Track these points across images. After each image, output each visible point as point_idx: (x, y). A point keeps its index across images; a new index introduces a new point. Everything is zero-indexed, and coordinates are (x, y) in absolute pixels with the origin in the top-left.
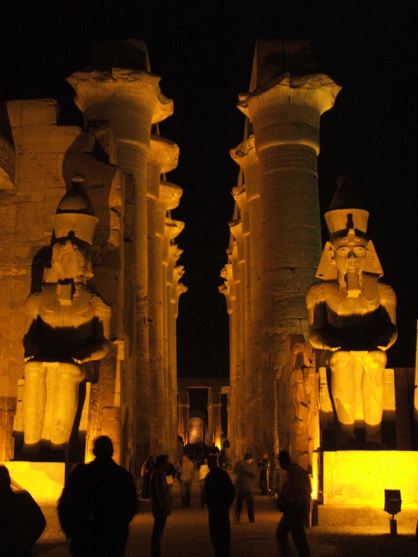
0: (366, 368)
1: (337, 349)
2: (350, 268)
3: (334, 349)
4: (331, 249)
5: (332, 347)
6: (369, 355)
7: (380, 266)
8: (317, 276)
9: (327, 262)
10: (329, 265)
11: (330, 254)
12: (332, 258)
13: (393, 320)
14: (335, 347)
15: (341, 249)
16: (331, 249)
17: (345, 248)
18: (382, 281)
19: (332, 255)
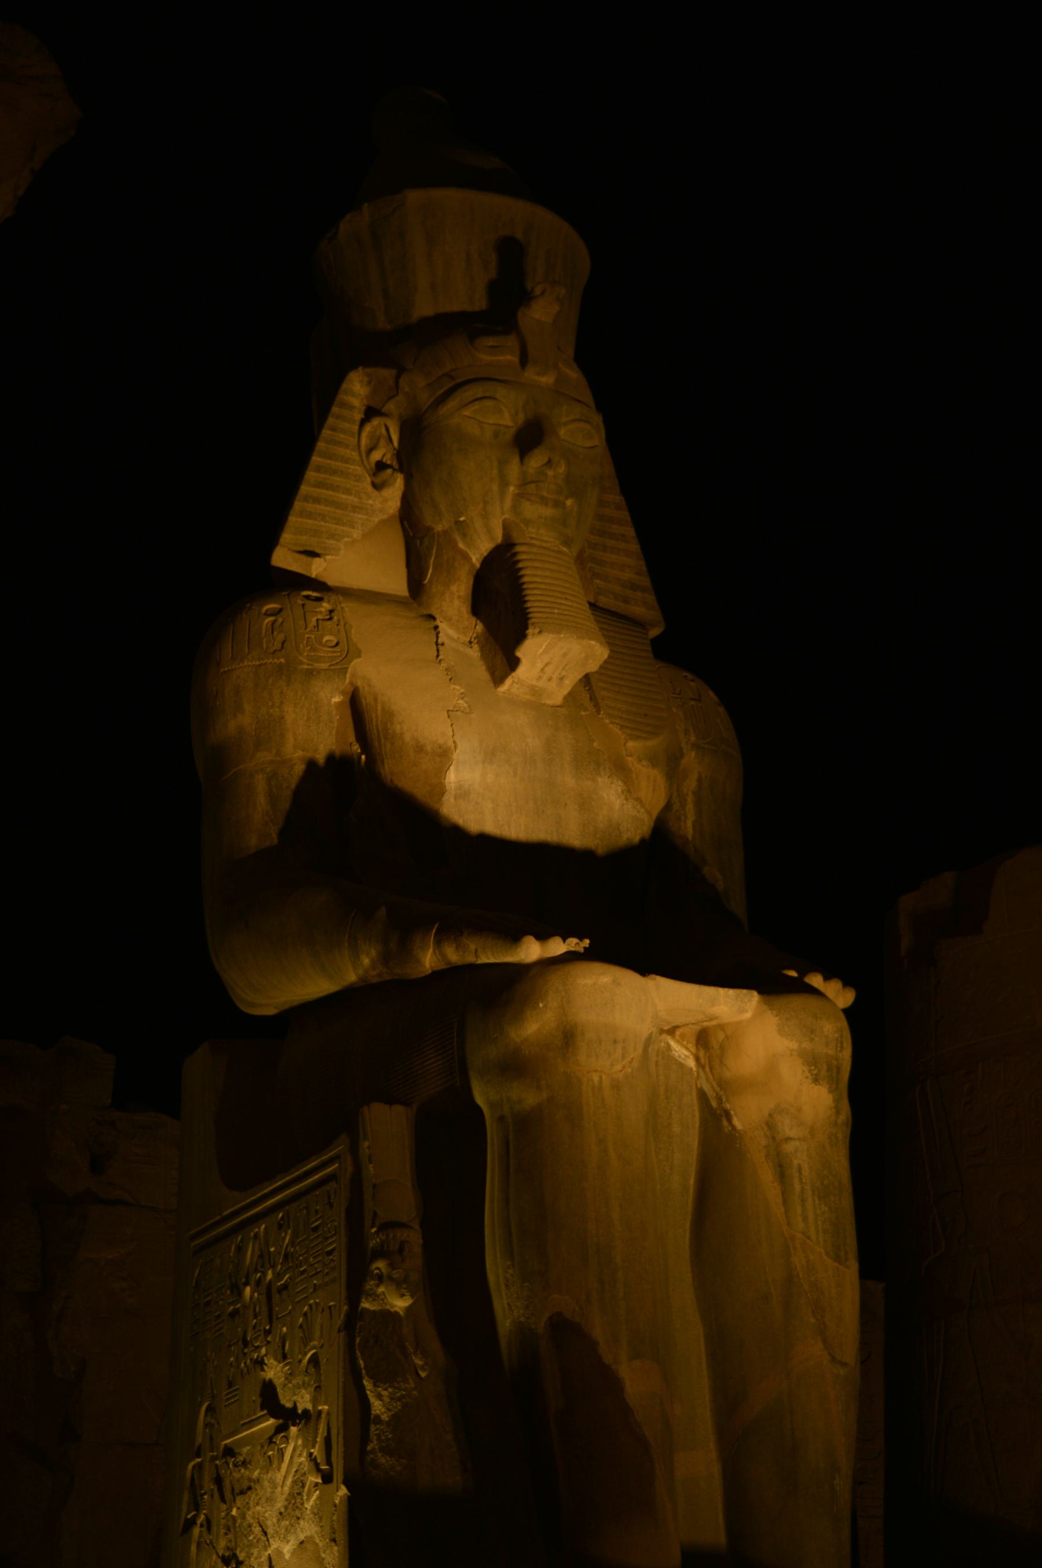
0: (746, 1115)
1: (557, 947)
2: (531, 510)
3: (531, 951)
4: (371, 413)
5: (515, 938)
6: (771, 1022)
7: (646, 581)
8: (283, 558)
9: (347, 491)
10: (355, 509)
11: (364, 441)
12: (381, 466)
13: (737, 904)
14: (542, 937)
15: (478, 390)
16: (371, 413)
17: (501, 391)
18: (664, 650)
19: (376, 456)
